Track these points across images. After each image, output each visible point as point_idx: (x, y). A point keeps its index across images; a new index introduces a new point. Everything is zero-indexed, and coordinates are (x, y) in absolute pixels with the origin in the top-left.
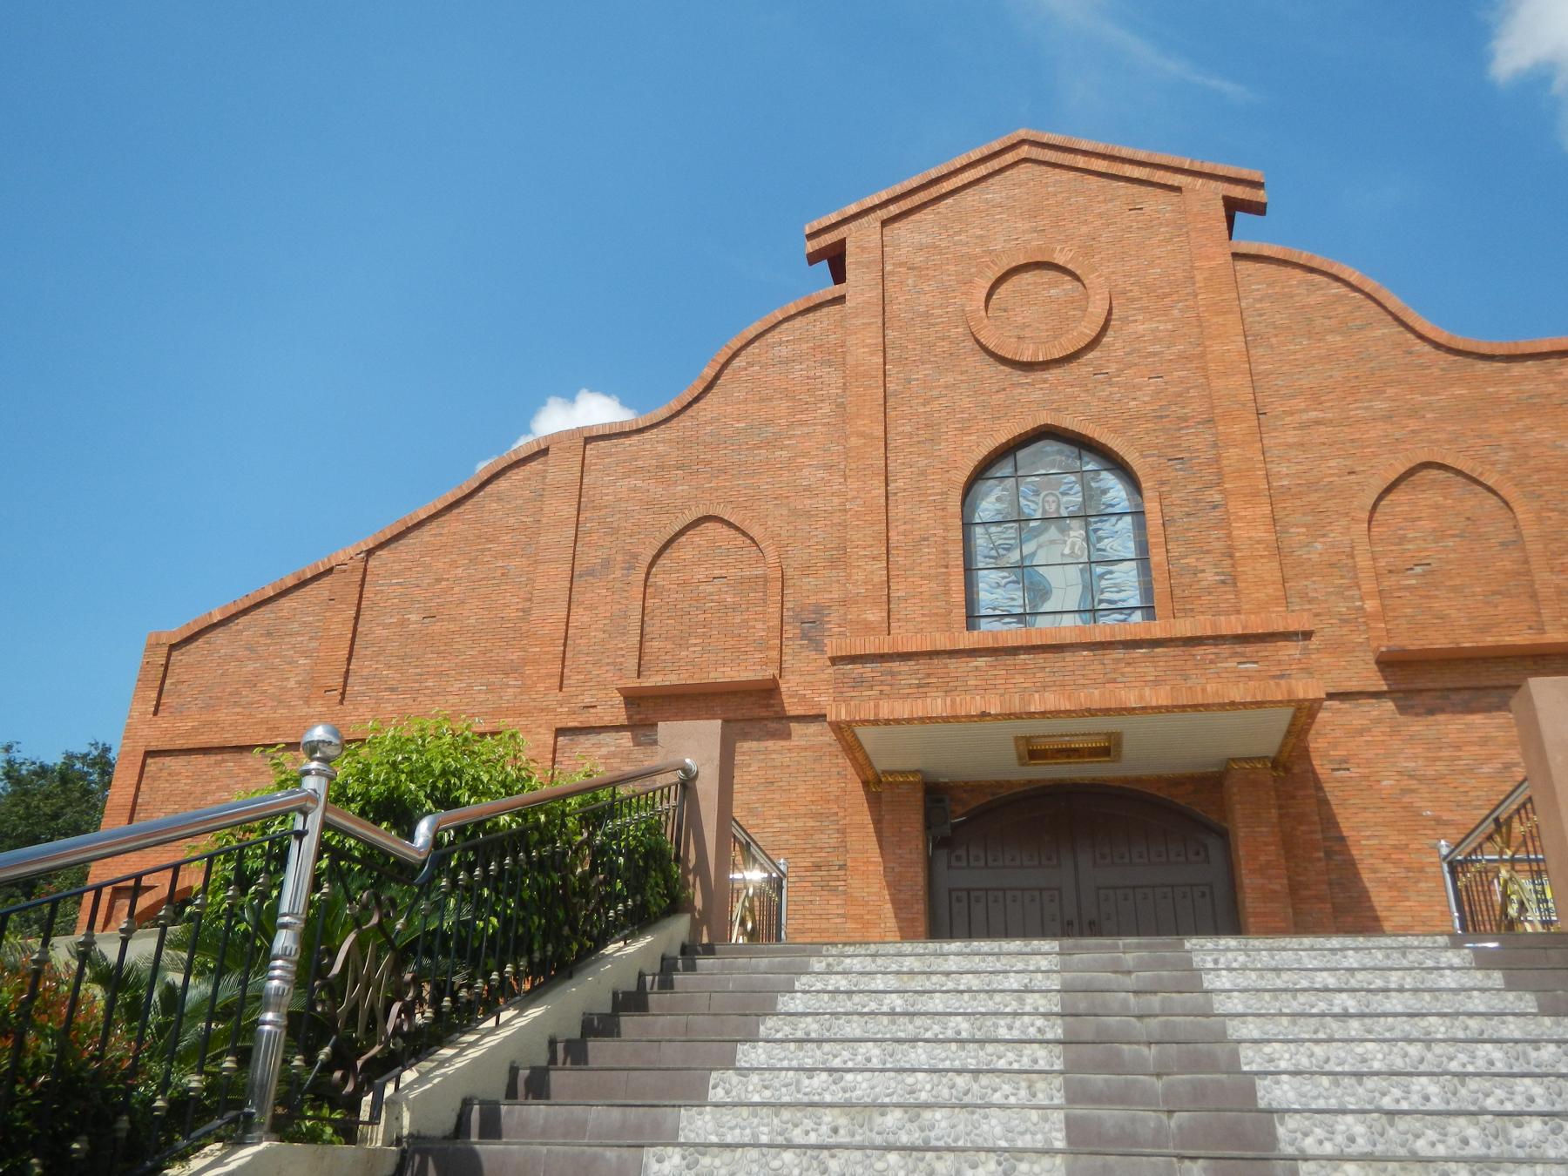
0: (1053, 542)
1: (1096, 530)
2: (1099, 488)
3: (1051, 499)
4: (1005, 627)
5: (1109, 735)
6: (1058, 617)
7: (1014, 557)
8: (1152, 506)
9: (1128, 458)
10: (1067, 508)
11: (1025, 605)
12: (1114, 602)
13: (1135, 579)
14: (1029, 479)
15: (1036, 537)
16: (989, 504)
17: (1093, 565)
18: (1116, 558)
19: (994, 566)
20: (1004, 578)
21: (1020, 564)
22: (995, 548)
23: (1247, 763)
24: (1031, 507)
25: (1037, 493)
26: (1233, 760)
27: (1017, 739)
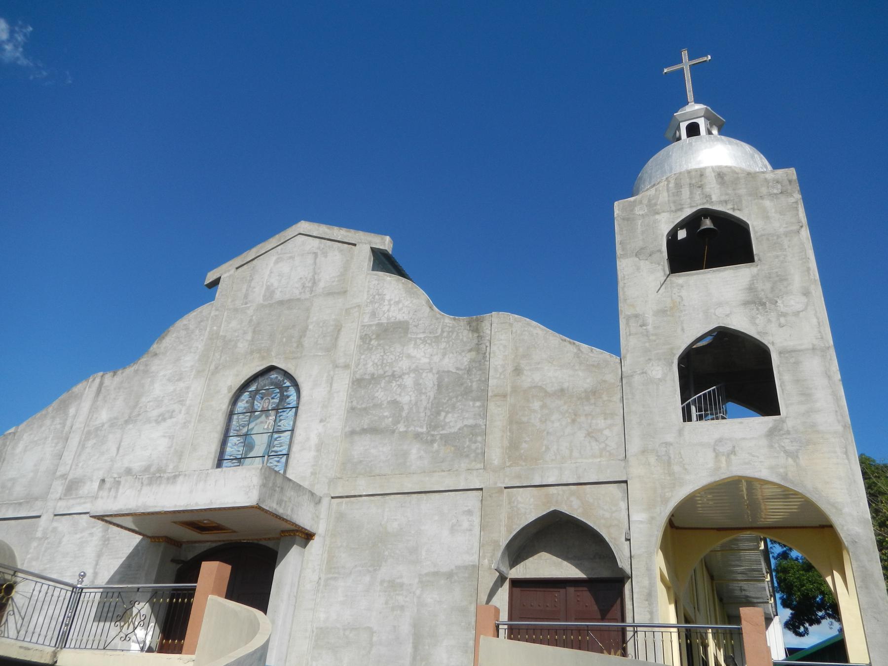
0: (262, 422)
2: (287, 395)
3: (267, 401)
4: (232, 465)
7: (245, 430)
11: (242, 455)
14: (261, 392)
15: (256, 420)
16: (242, 405)
17: (274, 434)
20: (238, 441)
22: (240, 425)
23: (287, 533)
24: (258, 405)
25: (262, 398)
26: (283, 532)
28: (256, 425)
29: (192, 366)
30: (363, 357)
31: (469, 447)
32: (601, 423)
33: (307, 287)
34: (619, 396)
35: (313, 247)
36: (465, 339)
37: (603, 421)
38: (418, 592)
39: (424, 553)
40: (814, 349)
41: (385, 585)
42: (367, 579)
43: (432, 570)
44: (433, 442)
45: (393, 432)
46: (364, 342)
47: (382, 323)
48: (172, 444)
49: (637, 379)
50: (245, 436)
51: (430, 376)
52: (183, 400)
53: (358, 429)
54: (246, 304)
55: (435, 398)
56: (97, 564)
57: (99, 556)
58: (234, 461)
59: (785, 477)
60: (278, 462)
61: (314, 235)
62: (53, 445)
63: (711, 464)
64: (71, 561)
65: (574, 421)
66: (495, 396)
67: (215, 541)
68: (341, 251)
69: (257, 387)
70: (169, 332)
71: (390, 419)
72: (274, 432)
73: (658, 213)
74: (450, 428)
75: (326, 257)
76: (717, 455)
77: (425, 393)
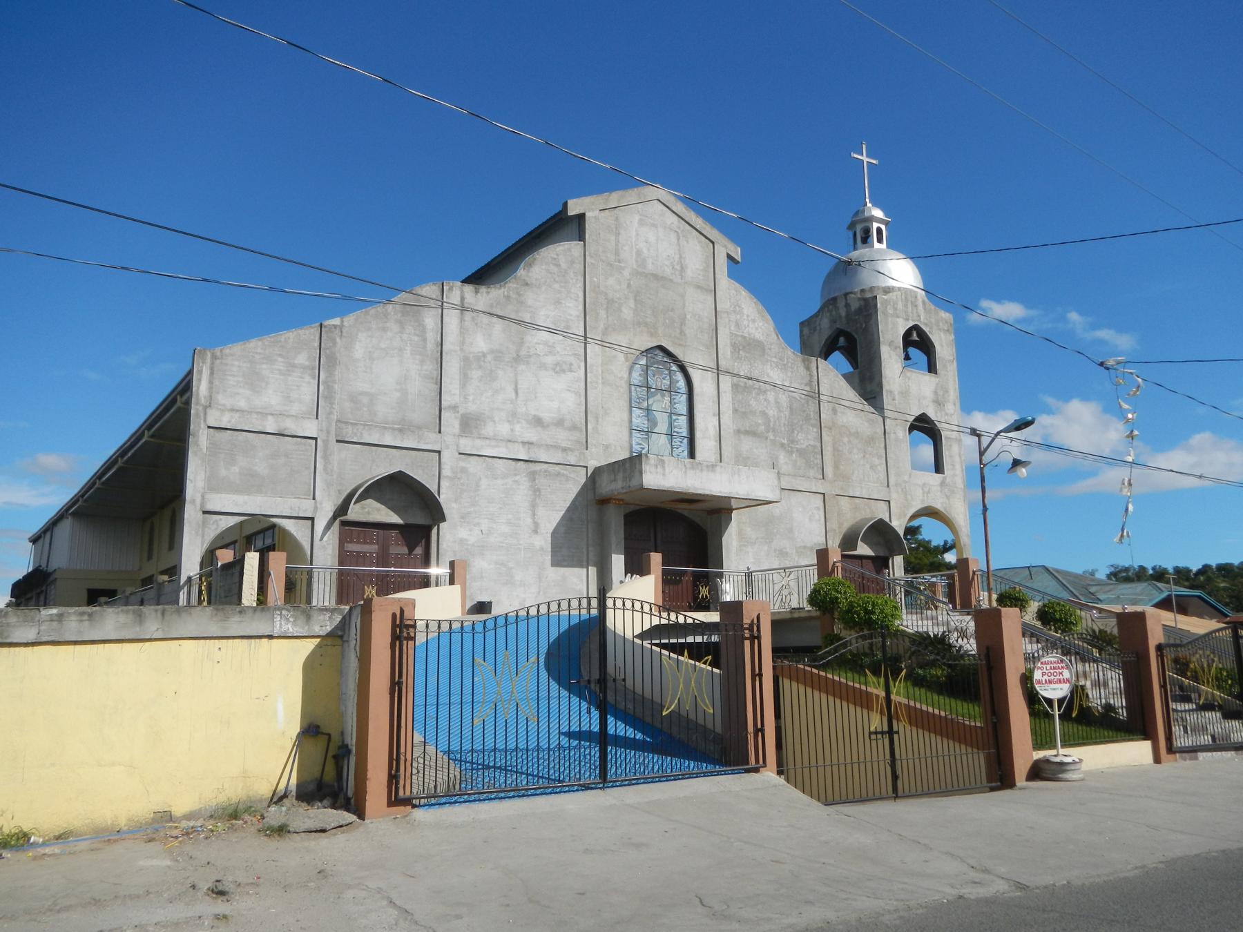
0: (659, 401)
1: (674, 399)
3: (659, 380)
7: (645, 404)
12: (678, 433)
15: (653, 396)
25: (654, 376)
28: (654, 402)
29: (578, 316)
30: (736, 364)
31: (813, 461)
32: (876, 461)
33: (677, 269)
34: (883, 445)
35: (673, 223)
36: (802, 374)
37: (876, 460)
38: (796, 559)
39: (796, 533)
40: (956, 439)
41: (777, 552)
42: (766, 548)
43: (802, 544)
44: (791, 453)
45: (767, 438)
46: (735, 350)
47: (745, 338)
48: (581, 402)
49: (892, 436)
51: (783, 396)
52: (579, 355)
53: (743, 429)
54: (619, 262)
55: (789, 418)
56: (534, 514)
57: (533, 506)
58: (642, 433)
59: (945, 509)
60: (681, 442)
61: (674, 209)
62: (417, 362)
63: (921, 498)
64: (501, 508)
65: (864, 456)
66: (825, 427)
67: (638, 505)
68: (699, 242)
70: (535, 259)
71: (763, 427)
73: (898, 317)
74: (801, 444)
75: (688, 242)
76: (923, 493)
77: (783, 412)
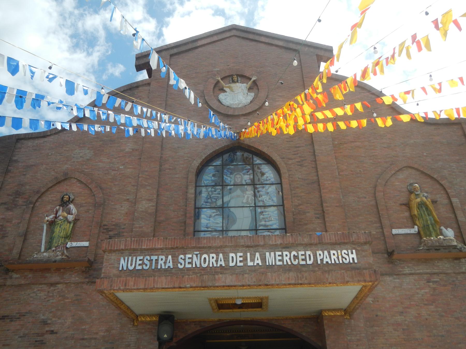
0: (238, 196)
3: (238, 176)
5: (262, 299)
6: (239, 232)
7: (219, 203)
8: (285, 181)
9: (274, 158)
10: (245, 181)
13: (277, 215)
14: (228, 167)
17: (257, 208)
18: (267, 205)
19: (209, 207)
20: (214, 213)
21: (222, 206)
24: (229, 179)
25: (231, 173)
26: (325, 310)
27: (210, 300)
50: (221, 209)
69: (223, 163)
72: (255, 206)
